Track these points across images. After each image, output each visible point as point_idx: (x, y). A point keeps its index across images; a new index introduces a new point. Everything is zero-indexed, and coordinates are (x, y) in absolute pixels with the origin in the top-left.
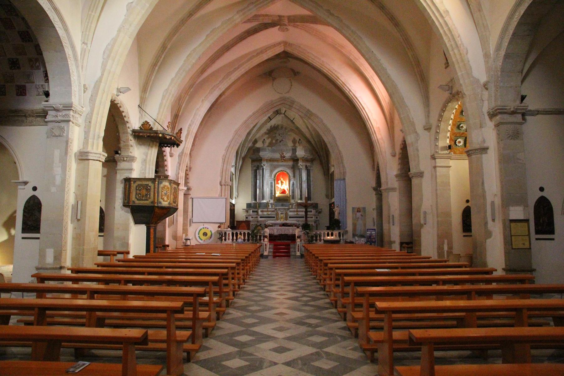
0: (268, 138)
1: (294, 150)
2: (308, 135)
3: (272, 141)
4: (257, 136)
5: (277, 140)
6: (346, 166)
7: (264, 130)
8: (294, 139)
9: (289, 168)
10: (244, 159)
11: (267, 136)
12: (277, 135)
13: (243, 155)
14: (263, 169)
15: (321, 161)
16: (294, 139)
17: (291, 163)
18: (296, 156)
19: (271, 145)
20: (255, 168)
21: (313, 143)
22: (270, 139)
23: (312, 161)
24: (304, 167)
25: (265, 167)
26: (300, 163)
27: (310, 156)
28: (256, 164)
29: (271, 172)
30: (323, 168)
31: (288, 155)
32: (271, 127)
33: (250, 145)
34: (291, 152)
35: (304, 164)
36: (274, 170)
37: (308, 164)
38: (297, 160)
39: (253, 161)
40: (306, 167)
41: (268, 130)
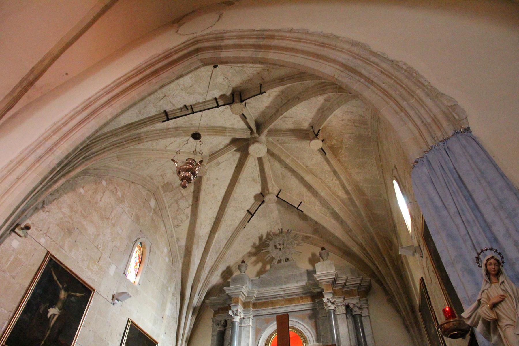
0: (256, 263)
1: (310, 274)
2: (338, 232)
3: (264, 267)
4: (232, 259)
5: (273, 258)
6: (441, 88)
7: (243, 246)
8: (314, 255)
9: (303, 320)
10: (199, 312)
11: (253, 259)
12: (271, 248)
13: (196, 301)
14: (233, 324)
15: (387, 292)
16: (314, 255)
17: (306, 305)
18: (316, 284)
19: (259, 273)
20: (219, 329)
21: (355, 249)
22: (259, 266)
23: (364, 292)
24: (342, 310)
25: (237, 319)
26: (327, 297)
27: (354, 281)
28: (221, 318)
29: (258, 332)
30: (398, 311)
31: (295, 286)
32: (260, 238)
33: (216, 279)
34: (305, 278)
35: (339, 300)
36: (264, 329)
37: (353, 301)
38: (320, 295)
39: (216, 312)
40: (347, 307)
41: (254, 246)
